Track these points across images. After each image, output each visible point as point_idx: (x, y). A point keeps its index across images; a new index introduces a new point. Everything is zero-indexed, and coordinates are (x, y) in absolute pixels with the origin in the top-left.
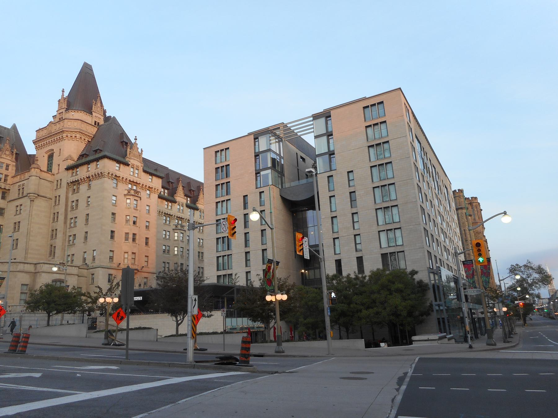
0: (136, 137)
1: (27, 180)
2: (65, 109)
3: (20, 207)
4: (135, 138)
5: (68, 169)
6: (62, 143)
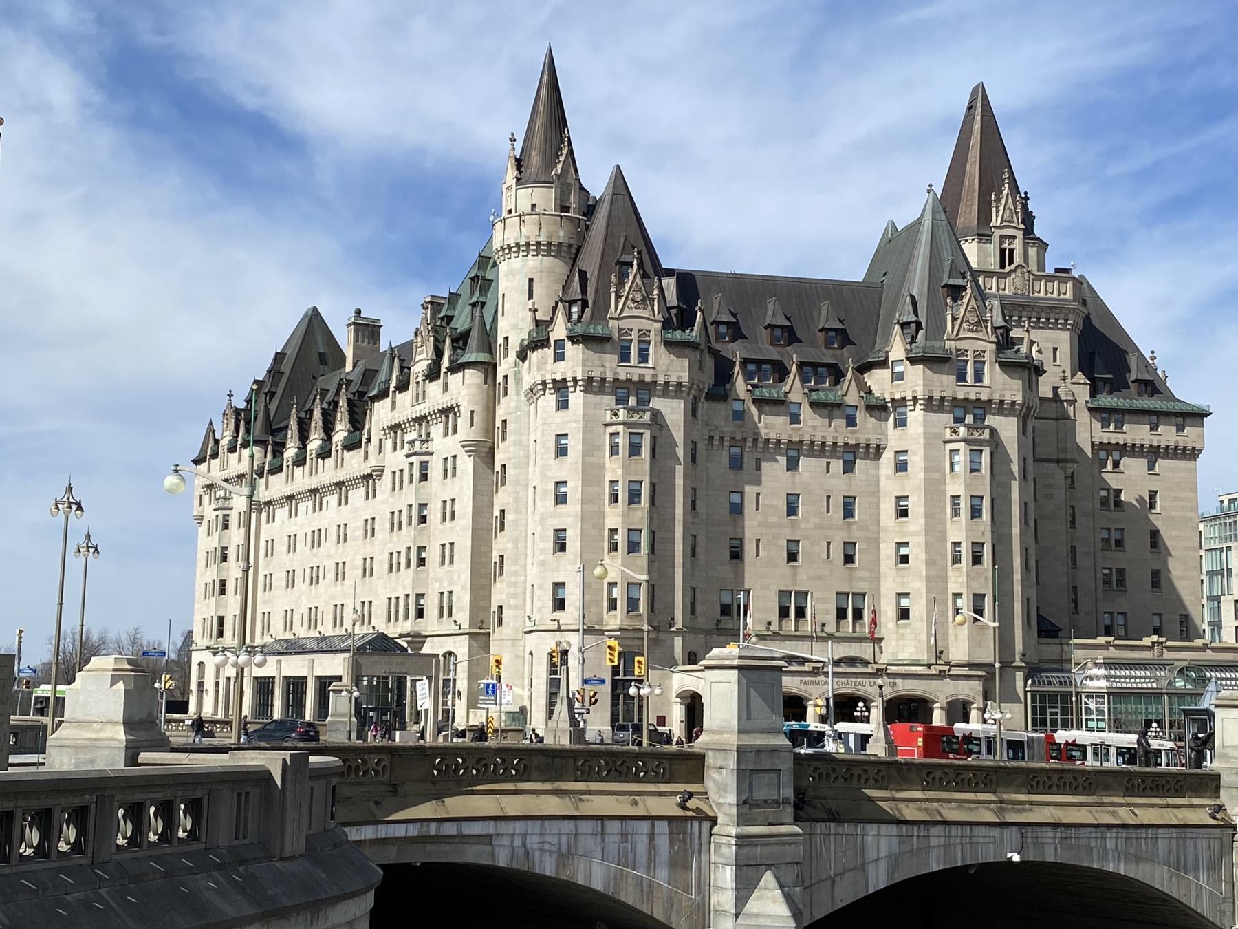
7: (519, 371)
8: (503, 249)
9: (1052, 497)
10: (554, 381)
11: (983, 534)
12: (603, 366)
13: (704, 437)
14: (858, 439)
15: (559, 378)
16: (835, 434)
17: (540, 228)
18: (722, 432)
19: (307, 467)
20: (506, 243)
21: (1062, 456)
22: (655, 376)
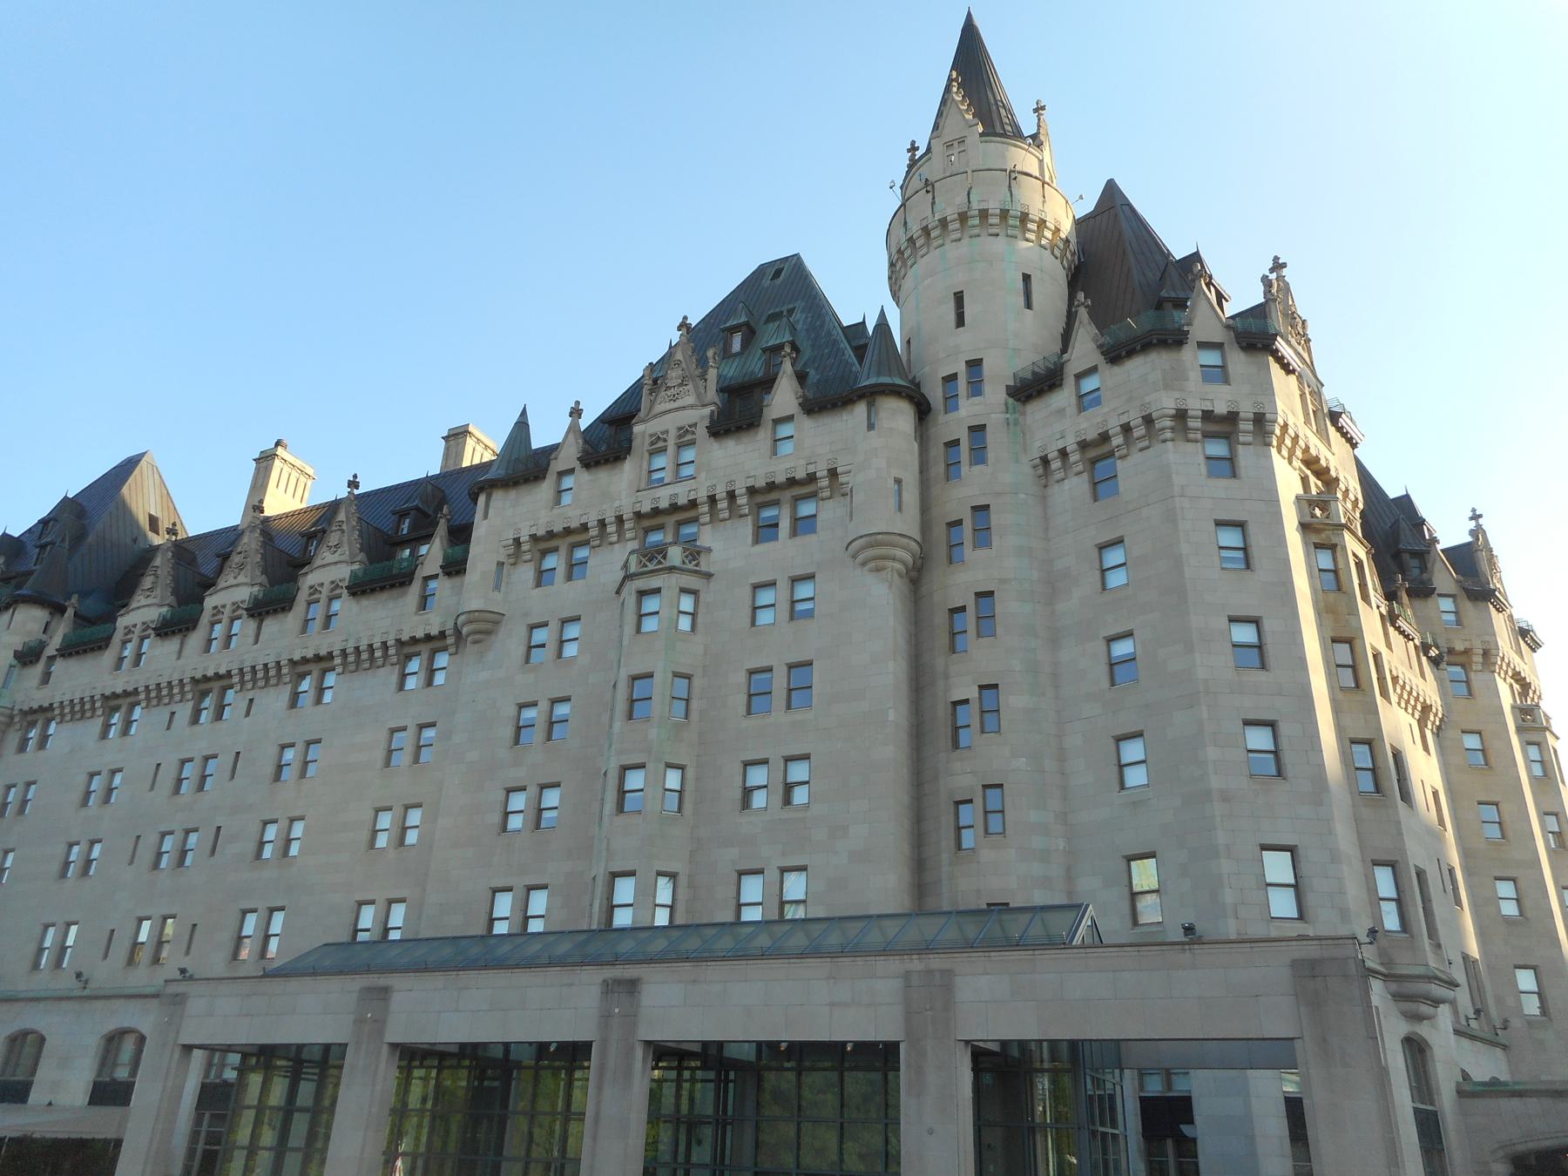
7: (1016, 423)
8: (963, 217)
10: (1207, 416)
15: (1221, 409)
17: (1044, 202)
19: (195, 639)
20: (975, 205)
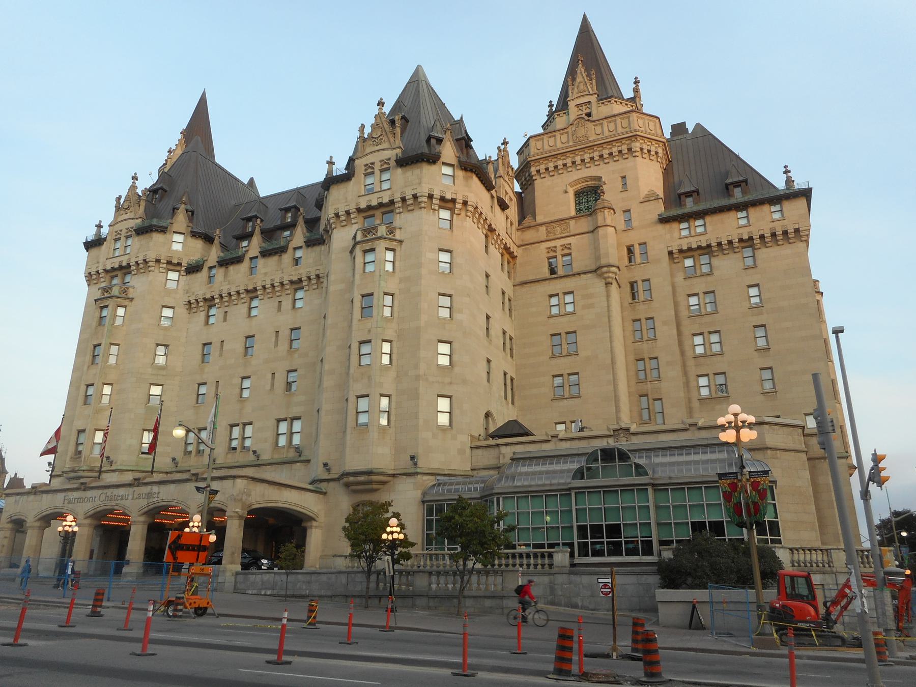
0: (786, 167)
1: (581, 236)
2: (596, 96)
3: (550, 300)
4: (784, 170)
5: (663, 220)
6: (630, 162)
9: (591, 306)
11: (369, 331)
12: (98, 263)
13: (185, 303)
14: (301, 274)
16: (282, 275)
18: (197, 295)
21: (598, 265)
22: (129, 259)
